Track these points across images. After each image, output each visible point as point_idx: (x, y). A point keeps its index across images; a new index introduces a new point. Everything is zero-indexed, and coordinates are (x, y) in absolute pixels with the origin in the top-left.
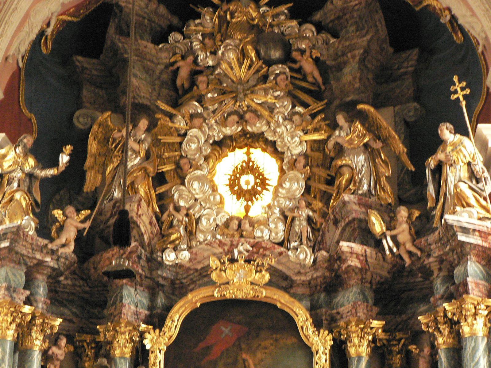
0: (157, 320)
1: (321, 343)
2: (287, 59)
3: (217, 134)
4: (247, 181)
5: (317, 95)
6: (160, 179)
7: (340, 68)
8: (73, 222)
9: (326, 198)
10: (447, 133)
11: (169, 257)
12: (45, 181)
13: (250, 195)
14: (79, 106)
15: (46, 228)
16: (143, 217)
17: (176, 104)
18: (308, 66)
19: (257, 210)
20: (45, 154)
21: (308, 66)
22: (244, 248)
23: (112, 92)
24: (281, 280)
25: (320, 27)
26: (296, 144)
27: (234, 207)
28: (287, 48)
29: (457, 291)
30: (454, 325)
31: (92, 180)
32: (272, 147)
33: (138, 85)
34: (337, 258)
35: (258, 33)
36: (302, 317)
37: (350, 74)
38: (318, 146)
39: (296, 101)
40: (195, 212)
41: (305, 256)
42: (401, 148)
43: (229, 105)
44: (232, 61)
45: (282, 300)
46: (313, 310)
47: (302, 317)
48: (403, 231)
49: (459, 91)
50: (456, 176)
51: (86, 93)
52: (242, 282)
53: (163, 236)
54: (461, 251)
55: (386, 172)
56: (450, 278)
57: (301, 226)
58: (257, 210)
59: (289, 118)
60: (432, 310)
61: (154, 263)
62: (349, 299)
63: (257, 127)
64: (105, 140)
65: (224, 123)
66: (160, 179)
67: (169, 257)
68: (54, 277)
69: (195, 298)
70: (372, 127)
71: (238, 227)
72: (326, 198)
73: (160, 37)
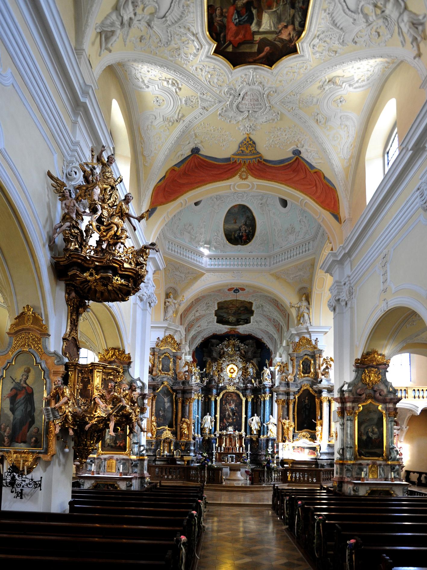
0: (218, 395)
1: (244, 400)
2: (239, 350)
3: (228, 363)
4: (232, 371)
5: (244, 357)
6: (218, 371)
7: (248, 352)
8: (206, 380)
9: (245, 376)
10: (265, 369)
11: (220, 385)
12: (201, 374)
13: (233, 373)
14: (204, 356)
15: (202, 381)
16: (216, 378)
17: (221, 358)
18: (243, 352)
19: (234, 375)
20: (202, 370)
21: (243, 352)
22: (232, 384)
23: (210, 355)
24: (238, 389)
25: (245, 344)
26: (241, 366)
27: (230, 375)
28: (239, 348)
29: (265, 393)
30: (264, 398)
31: (208, 371)
32: (237, 366)
33: (215, 355)
34: (246, 386)
35: (234, 345)
36: (241, 395)
37: (250, 354)
38: (244, 367)
39: (241, 358)
40: (225, 377)
41: (242, 385)
42: (257, 368)
43: (230, 359)
44: (230, 350)
45: (238, 392)
46: (242, 393)
47: (241, 395)
48: (257, 382)
49: (267, 362)
50: (265, 376)
51: (205, 354)
52: (231, 389)
53: (219, 381)
54: (266, 387)
55: (255, 372)
56: (264, 390)
57: (241, 380)
58: (234, 375)
59: (240, 361)
60: (261, 395)
61: (218, 386)
62: (248, 392)
63: (234, 362)
64: (210, 365)
65: (229, 362)
66: (218, 371)
67: (220, 385)
68: (202, 389)
69: (224, 391)
70: (253, 364)
71: (231, 379)
72: (245, 376)
73: (218, 345)
